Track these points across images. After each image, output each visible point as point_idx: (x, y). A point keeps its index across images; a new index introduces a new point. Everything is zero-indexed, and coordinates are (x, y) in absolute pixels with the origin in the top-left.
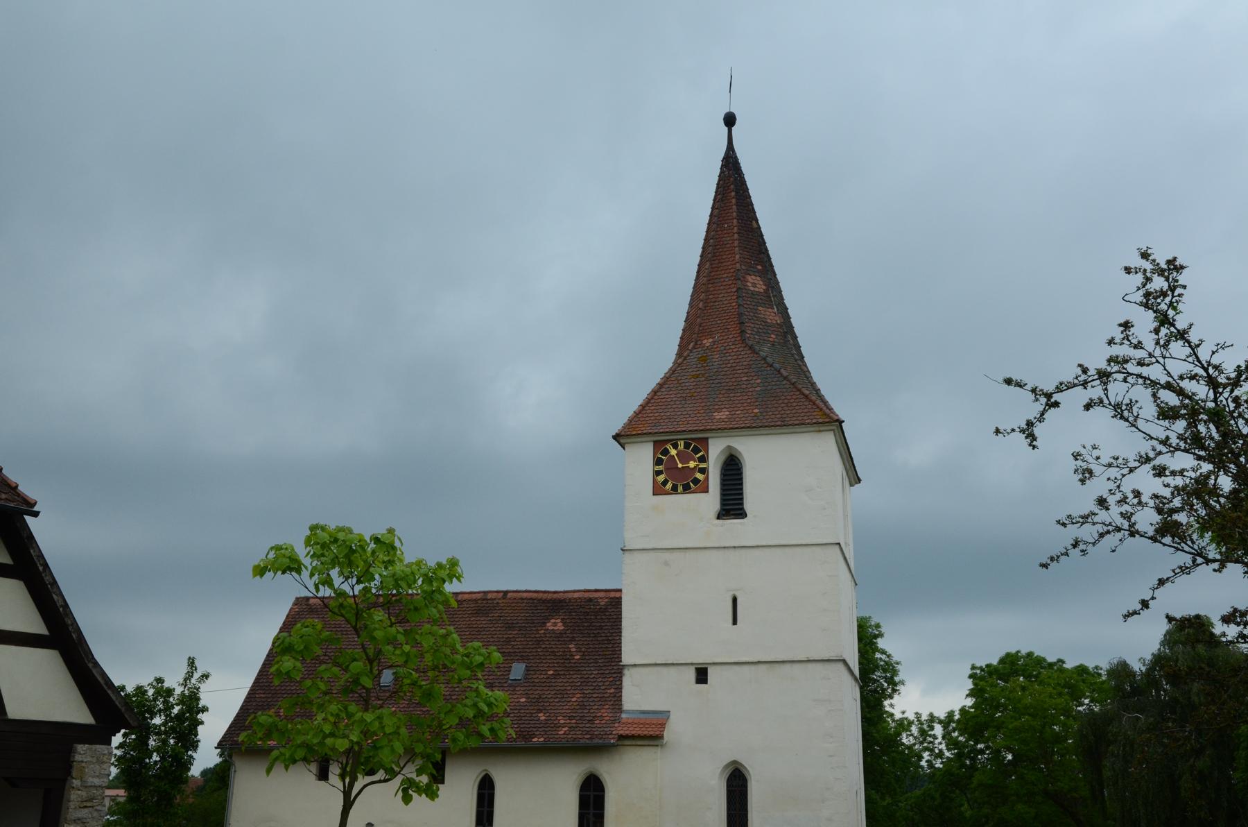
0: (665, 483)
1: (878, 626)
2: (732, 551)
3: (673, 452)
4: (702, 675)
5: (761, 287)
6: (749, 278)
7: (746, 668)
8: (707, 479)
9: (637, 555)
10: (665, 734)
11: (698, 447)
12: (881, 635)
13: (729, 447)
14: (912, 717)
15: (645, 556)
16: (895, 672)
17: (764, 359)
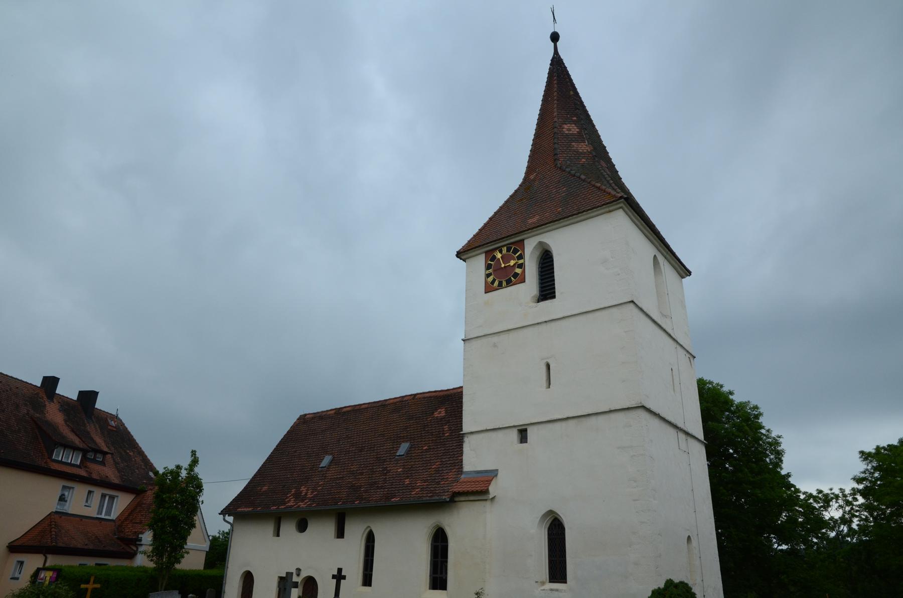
0: (494, 281)
1: (756, 407)
2: (544, 326)
3: (499, 256)
4: (523, 434)
5: (575, 129)
6: (565, 126)
7: (557, 426)
8: (524, 271)
9: (474, 342)
10: (491, 489)
11: (517, 249)
12: (760, 414)
13: (541, 243)
14: (837, 492)
15: (479, 341)
16: (778, 444)
17: (569, 172)
